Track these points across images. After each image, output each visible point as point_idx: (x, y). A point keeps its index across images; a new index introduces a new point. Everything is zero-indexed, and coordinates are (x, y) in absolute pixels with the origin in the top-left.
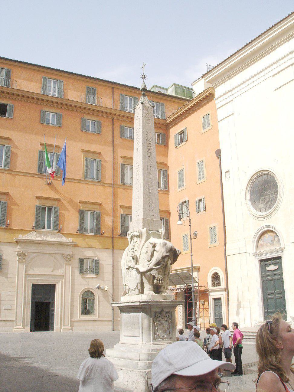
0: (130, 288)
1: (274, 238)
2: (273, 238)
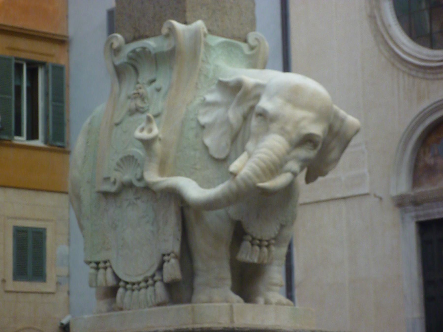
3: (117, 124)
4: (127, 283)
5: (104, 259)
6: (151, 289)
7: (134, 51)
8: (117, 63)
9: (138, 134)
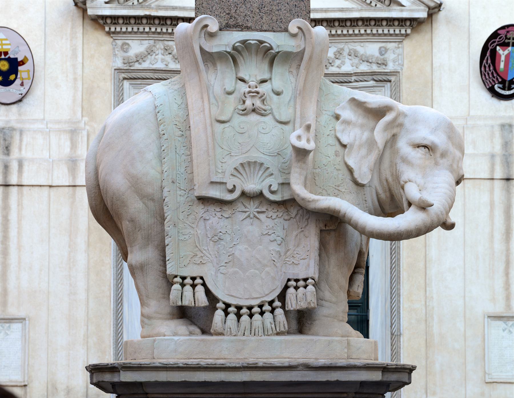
4: (228, 306)
6: (268, 315)
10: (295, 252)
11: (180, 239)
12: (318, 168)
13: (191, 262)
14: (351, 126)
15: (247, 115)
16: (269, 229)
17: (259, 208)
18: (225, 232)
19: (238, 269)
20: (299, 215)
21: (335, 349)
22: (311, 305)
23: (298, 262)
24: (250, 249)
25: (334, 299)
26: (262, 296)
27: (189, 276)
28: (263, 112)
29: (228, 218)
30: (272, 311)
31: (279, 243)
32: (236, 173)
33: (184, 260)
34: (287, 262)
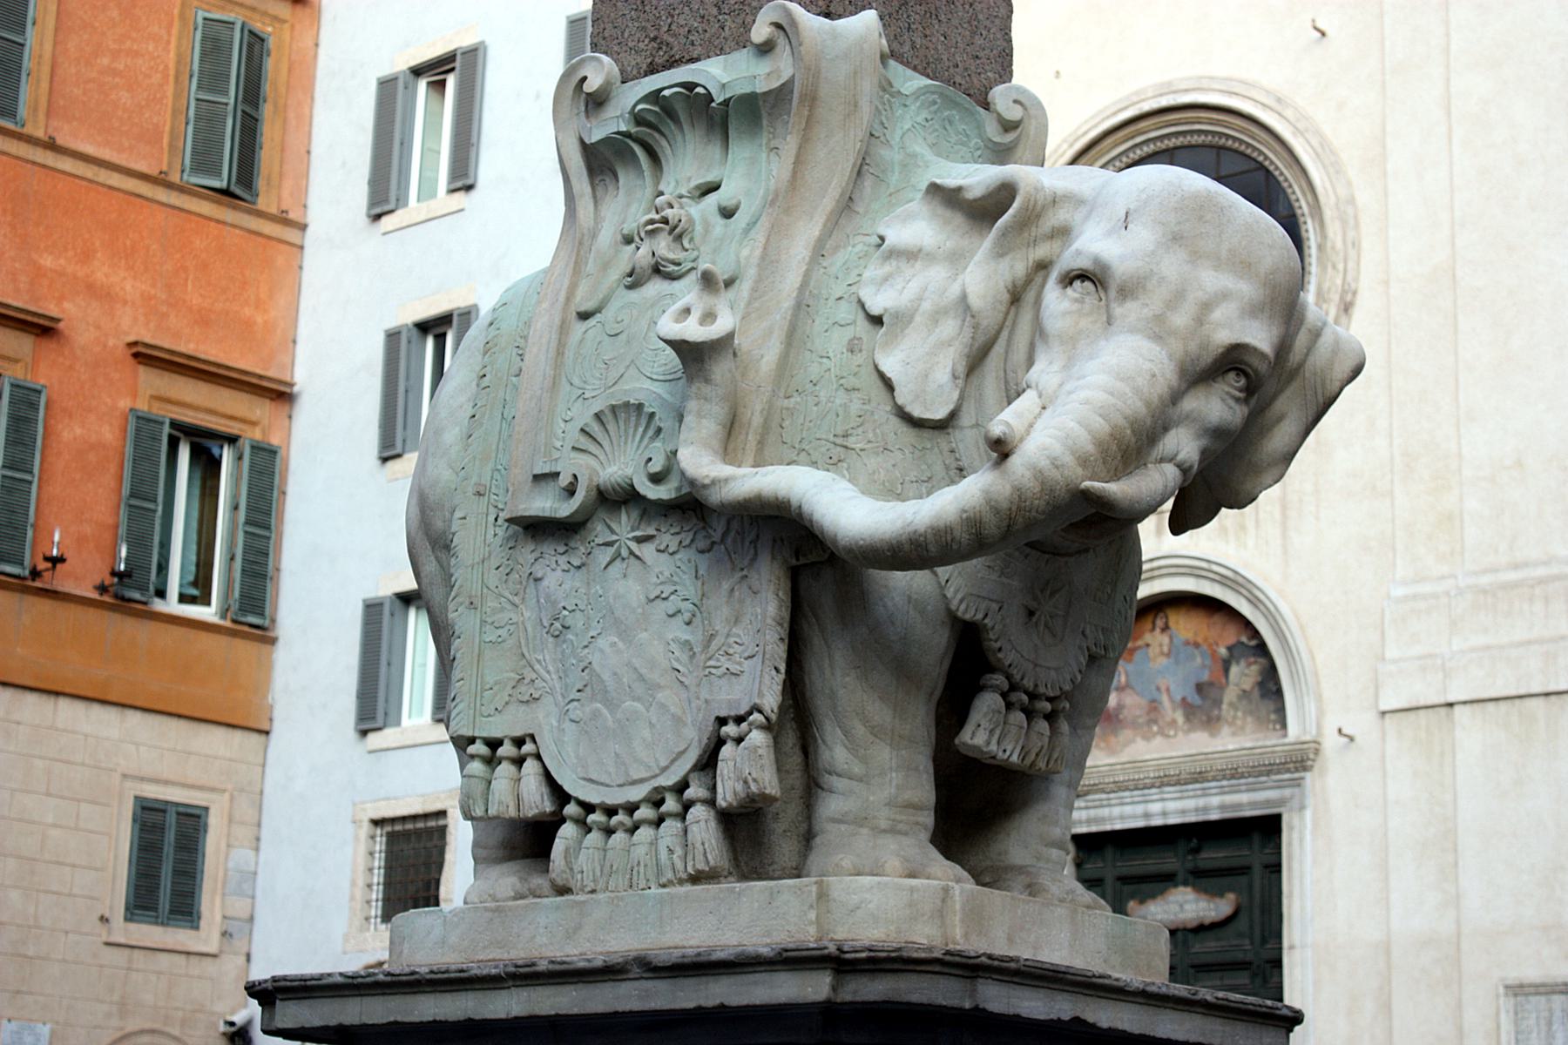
0: (560, 796)
1: (1226, 666)
2: (1220, 666)
3: (584, 316)
4: (589, 808)
5: (518, 733)
6: (672, 826)
7: (655, 96)
8: (596, 136)
9: (670, 327)
10: (732, 640)
11: (487, 640)
12: (795, 394)
13: (512, 699)
14: (918, 265)
15: (642, 285)
16: (661, 583)
17: (642, 527)
18: (574, 607)
19: (599, 705)
20: (732, 534)
21: (784, 914)
22: (749, 788)
23: (739, 668)
24: (621, 645)
25: (857, 769)
26: (653, 774)
27: (506, 737)
28: (672, 268)
29: (579, 567)
30: (682, 816)
31: (687, 620)
32: (584, 442)
33: (496, 695)
34: (713, 671)
